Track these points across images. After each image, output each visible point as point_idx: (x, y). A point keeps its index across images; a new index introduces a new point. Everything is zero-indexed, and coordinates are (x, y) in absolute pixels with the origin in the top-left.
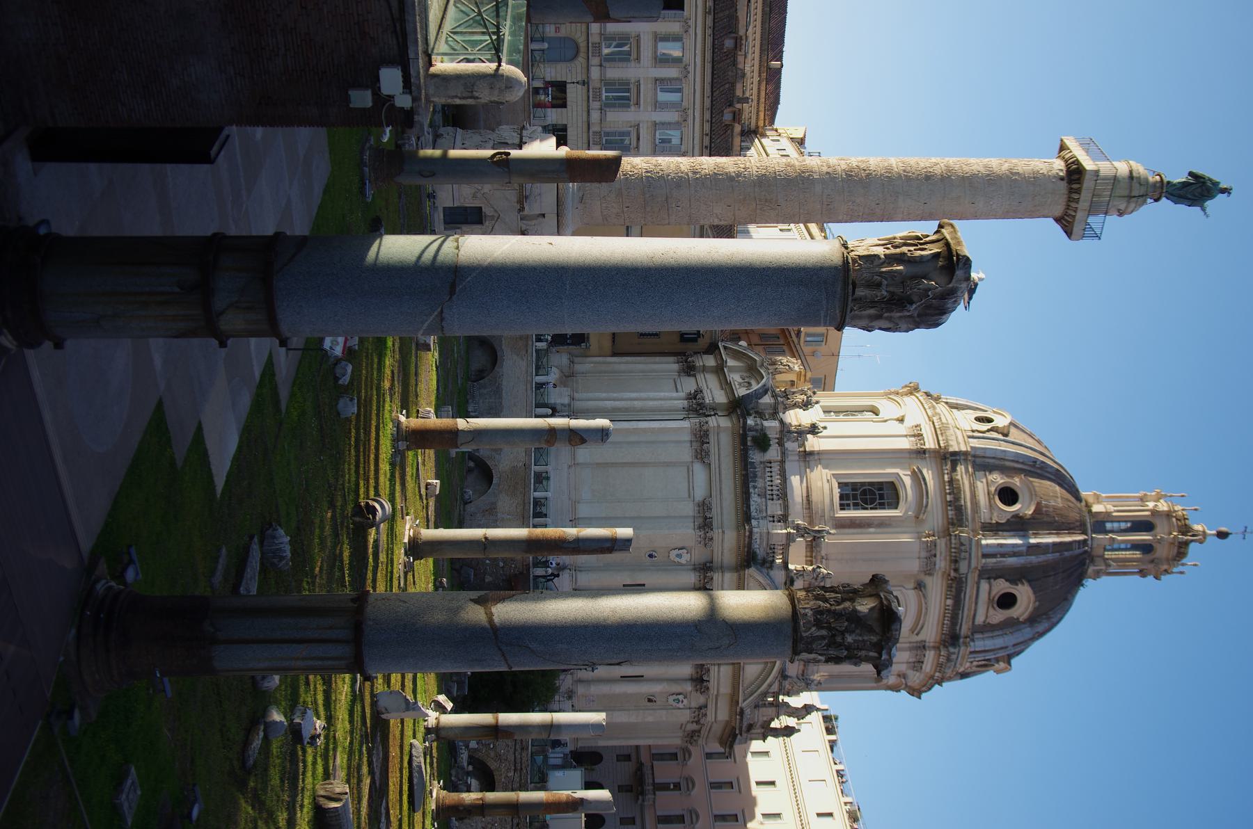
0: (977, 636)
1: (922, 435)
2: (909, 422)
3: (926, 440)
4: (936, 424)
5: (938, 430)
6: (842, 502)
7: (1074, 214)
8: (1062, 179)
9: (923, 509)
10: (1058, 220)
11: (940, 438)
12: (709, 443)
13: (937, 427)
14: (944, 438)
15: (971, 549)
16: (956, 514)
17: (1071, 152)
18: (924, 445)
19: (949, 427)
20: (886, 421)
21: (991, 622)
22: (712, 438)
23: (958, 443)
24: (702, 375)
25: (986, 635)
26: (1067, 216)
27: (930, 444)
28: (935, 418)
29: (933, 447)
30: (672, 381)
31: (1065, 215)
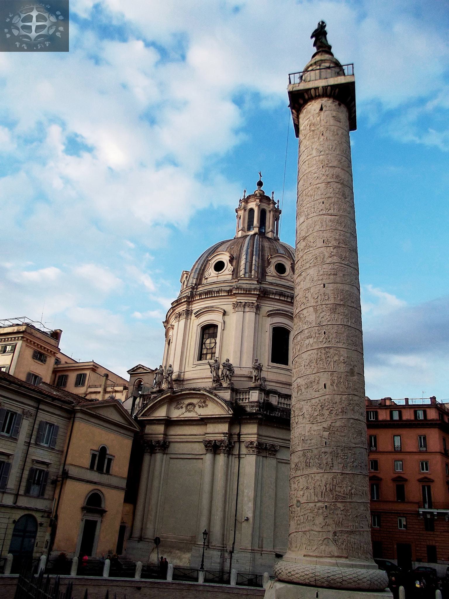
2: (229, 308)
4: (240, 292)
8: (340, 105)
12: (266, 444)
24: (170, 437)
28: (234, 292)
30: (172, 461)
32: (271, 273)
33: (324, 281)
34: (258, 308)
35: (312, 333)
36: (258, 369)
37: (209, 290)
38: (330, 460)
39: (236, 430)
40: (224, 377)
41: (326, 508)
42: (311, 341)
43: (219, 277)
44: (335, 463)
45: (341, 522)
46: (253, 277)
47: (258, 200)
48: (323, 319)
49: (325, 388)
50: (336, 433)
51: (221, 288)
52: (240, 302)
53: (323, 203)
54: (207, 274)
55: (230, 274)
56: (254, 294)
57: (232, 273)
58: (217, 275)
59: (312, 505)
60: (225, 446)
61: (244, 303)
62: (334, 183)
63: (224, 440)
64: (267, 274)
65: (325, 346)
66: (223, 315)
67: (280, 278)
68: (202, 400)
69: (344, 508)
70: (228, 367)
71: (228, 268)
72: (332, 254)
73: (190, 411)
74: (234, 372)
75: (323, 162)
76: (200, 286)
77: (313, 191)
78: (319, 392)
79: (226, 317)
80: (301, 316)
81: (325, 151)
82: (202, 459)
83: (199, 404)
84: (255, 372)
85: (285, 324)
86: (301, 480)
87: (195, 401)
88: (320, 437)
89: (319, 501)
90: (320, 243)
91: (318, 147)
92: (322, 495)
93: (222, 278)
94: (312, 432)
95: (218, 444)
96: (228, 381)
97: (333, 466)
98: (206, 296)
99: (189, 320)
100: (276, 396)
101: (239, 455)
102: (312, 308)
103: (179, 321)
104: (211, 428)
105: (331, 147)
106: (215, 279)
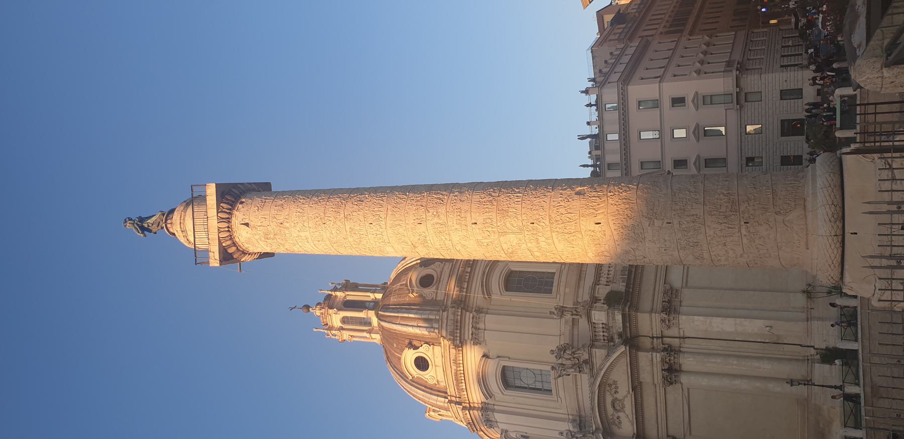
4: (458, 335)
5: (459, 328)
6: (552, 280)
8: (242, 203)
11: (459, 317)
12: (663, 302)
13: (458, 331)
19: (450, 335)
20: (498, 357)
22: (659, 305)
28: (458, 342)
32: (433, 293)
33: (469, 223)
34: (479, 311)
35: (532, 238)
36: (563, 311)
37: (454, 378)
38: (688, 219)
39: (647, 342)
40: (574, 358)
41: (748, 223)
42: (541, 239)
44: (693, 212)
45: (762, 206)
46: (437, 317)
47: (331, 311)
48: (515, 225)
49: (600, 223)
50: (655, 211)
51: (452, 361)
52: (472, 334)
53: (371, 224)
54: (432, 381)
55: (433, 348)
56: (461, 316)
57: (432, 346)
58: (434, 367)
59: (745, 241)
60: (669, 356)
61: (473, 329)
62: (346, 210)
63: (662, 358)
64: (434, 298)
65: (547, 223)
66: (489, 358)
67: (440, 281)
68: (608, 388)
69: (745, 202)
70: (561, 351)
71: (424, 351)
72: (435, 213)
73: (623, 407)
74: (567, 344)
75: (317, 223)
76: (448, 391)
77: (354, 236)
78: (605, 231)
79: (491, 355)
80: (510, 251)
81: (304, 221)
82: (688, 389)
83: (613, 392)
84: (567, 315)
85: (501, 274)
86: (715, 253)
87: (609, 399)
88: (660, 229)
89: (740, 231)
90: (422, 228)
91: (298, 229)
92: (732, 228)
93: (439, 361)
94: (655, 239)
95: (666, 367)
96: (579, 352)
97: (697, 215)
98: (462, 383)
99: (495, 407)
100: (599, 288)
101: (680, 338)
102: (502, 239)
103: (497, 422)
104: (645, 376)
105: (299, 213)
106: (439, 370)
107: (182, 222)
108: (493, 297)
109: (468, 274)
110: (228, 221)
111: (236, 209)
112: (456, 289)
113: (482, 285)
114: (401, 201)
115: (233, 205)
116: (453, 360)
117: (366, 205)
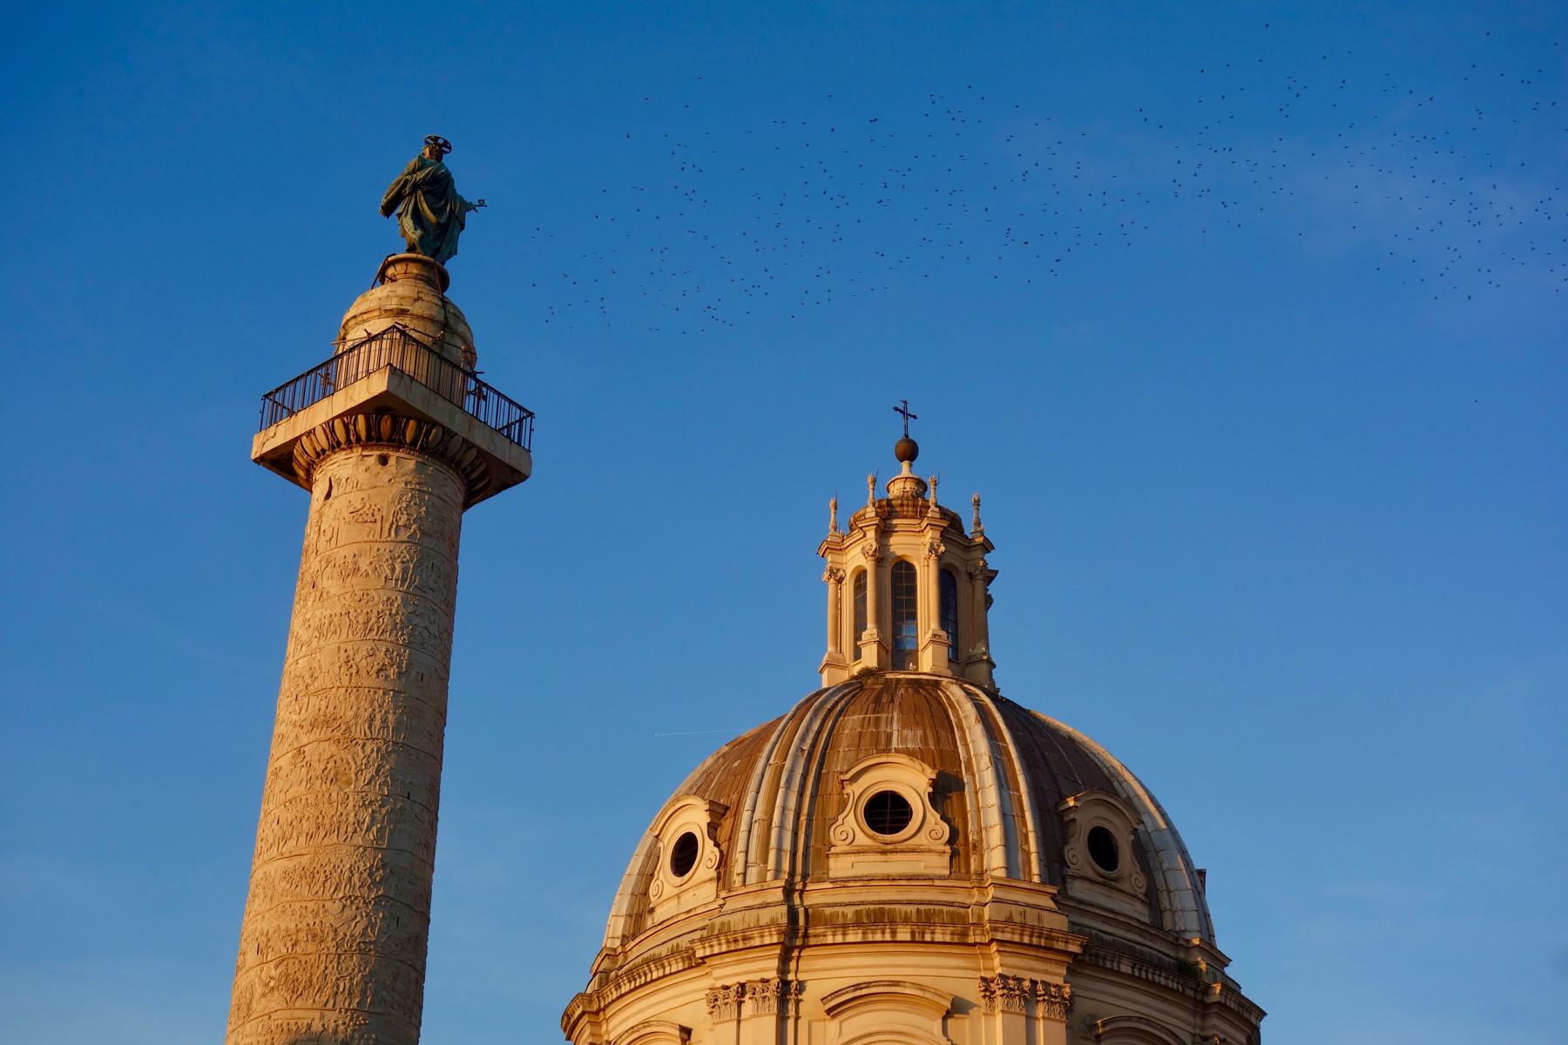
0: (1168, 925)
1: (743, 985)
3: (757, 977)
4: (716, 950)
7: (474, 452)
8: (384, 461)
9: (928, 995)
10: (472, 497)
11: (757, 942)
13: (724, 948)
14: (755, 933)
15: (1016, 903)
16: (943, 924)
17: (309, 433)
18: (768, 981)
21: (1143, 890)
23: (766, 905)
25: (1165, 904)
26: (473, 471)
27: (766, 967)
28: (700, 954)
29: (775, 963)
31: (467, 476)
34: (786, 992)
43: (684, 898)
51: (674, 942)
52: (726, 988)
57: (714, 874)
58: (677, 891)
67: (884, 852)
72: (272, 984)
85: (900, 1033)
107: (360, 319)
108: (833, 1025)
109: (888, 937)
110: (335, 446)
111: (365, 453)
112: (850, 911)
113: (857, 987)
114: (319, 884)
115: (373, 439)
116: (678, 945)
117: (320, 795)
